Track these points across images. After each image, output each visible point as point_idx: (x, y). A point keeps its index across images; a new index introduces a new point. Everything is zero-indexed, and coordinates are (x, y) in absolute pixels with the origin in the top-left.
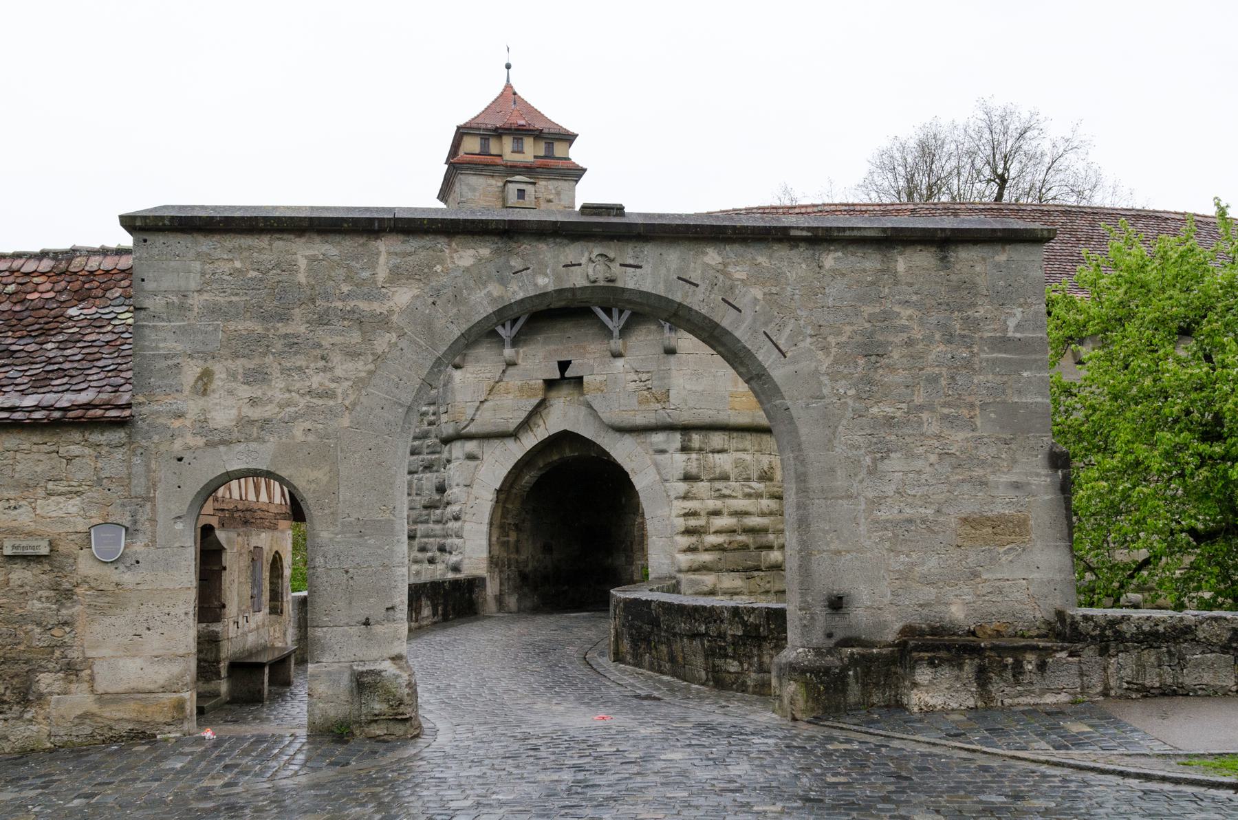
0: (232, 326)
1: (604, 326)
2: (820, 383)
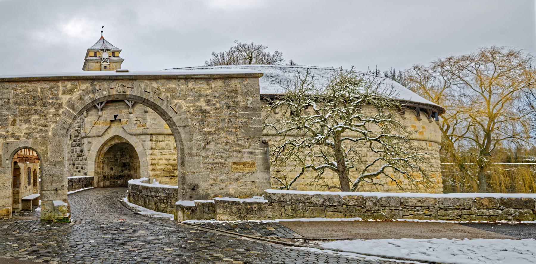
0: (21, 107)
1: (127, 105)
2: (188, 121)
